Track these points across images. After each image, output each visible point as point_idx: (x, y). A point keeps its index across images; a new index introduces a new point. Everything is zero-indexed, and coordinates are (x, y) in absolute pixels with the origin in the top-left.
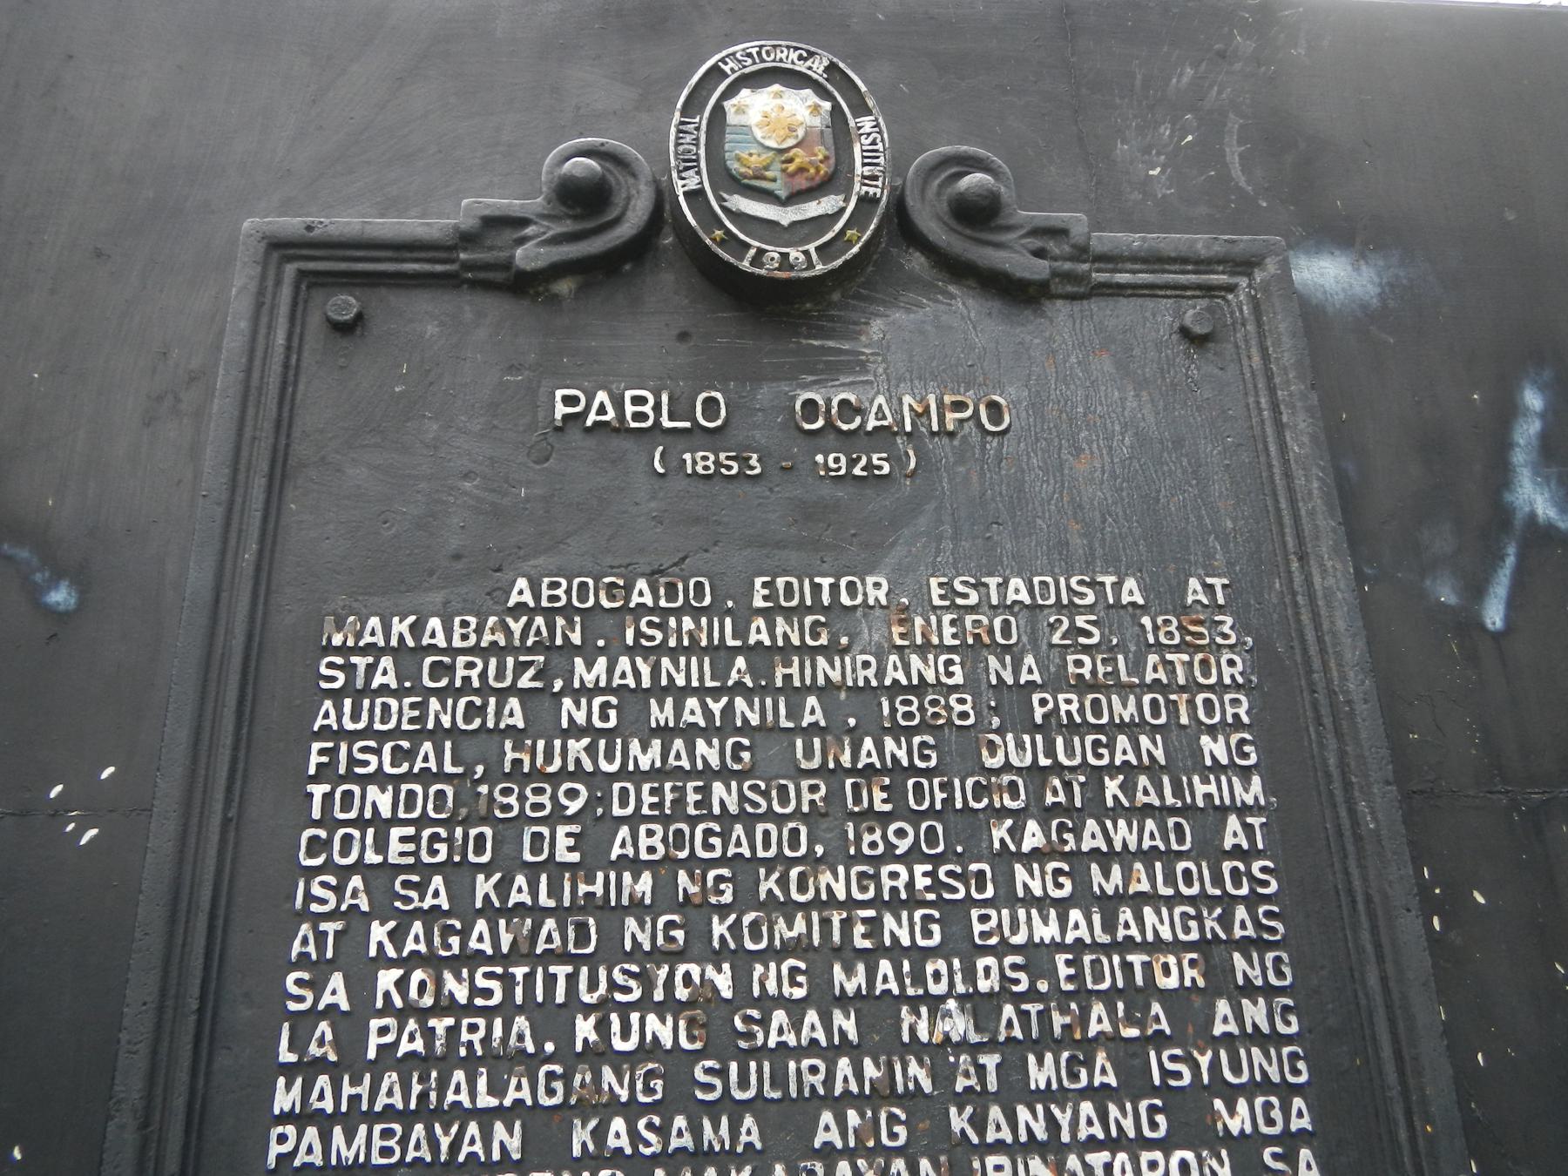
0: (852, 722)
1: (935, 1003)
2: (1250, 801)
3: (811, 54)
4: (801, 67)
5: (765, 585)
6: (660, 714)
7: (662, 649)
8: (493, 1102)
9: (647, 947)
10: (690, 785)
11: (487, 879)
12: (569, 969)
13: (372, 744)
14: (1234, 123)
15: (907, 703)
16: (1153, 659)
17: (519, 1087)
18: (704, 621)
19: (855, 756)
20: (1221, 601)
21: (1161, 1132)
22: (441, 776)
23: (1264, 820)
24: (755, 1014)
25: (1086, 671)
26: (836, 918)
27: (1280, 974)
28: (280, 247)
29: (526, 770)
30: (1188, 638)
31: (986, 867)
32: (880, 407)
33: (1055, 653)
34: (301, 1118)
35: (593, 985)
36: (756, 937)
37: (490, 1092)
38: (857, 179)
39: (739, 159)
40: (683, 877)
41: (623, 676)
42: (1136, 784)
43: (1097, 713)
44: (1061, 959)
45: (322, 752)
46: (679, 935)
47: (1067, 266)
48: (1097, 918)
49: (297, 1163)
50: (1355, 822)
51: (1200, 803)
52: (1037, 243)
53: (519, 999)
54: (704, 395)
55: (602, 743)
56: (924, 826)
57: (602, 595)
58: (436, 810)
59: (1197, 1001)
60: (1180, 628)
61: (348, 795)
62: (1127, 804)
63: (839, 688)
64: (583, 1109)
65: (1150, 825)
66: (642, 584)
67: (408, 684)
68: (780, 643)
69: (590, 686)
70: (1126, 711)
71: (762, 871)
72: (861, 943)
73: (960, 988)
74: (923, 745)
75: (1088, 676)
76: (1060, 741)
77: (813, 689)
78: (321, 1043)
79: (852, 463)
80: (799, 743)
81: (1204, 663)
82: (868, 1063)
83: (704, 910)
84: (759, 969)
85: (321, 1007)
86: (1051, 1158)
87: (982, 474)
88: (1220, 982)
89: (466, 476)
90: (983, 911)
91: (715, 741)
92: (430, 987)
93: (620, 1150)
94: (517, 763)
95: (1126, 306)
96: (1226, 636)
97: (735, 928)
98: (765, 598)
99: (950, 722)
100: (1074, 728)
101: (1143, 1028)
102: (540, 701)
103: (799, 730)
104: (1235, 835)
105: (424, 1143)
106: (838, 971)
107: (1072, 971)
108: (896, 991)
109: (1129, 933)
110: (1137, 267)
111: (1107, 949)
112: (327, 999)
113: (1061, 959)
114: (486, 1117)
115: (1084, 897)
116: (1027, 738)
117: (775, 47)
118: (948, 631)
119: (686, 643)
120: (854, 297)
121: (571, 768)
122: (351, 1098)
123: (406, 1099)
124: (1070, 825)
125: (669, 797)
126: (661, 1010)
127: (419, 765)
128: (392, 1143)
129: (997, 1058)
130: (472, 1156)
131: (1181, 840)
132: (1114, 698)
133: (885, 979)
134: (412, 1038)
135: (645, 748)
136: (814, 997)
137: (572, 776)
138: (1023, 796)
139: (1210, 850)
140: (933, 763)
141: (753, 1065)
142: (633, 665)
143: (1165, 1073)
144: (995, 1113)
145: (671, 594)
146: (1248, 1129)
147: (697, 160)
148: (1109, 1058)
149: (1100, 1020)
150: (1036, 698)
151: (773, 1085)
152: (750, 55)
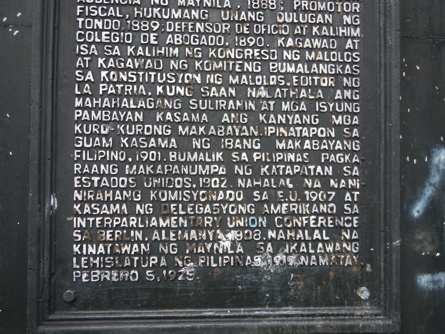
0: (239, 7)
1: (258, 87)
2: (355, 35)
8: (135, 107)
9: (177, 68)
11: (131, 47)
12: (155, 73)
13: (95, 7)
17: (142, 103)
21: (317, 123)
22: (116, 17)
23: (359, 41)
24: (207, 88)
26: (231, 63)
27: (356, 84)
29: (141, 16)
31: (275, 51)
34: (83, 108)
35: (161, 78)
36: (208, 67)
37: (134, 104)
40: (187, 50)
42: (322, 29)
43: (313, 7)
44: (294, 77)
45: (81, 9)
46: (186, 65)
49: (83, 119)
50: (385, 42)
51: (341, 35)
53: (141, 81)
55: (164, 10)
56: (258, 38)
58: (115, 27)
59: (332, 90)
61: (89, 22)
64: (159, 110)
65: (325, 41)
71: (210, 49)
72: (238, 70)
74: (260, 14)
76: (301, 15)
78: (87, 89)
80: (223, 12)
83: (194, 59)
84: (208, 76)
85: (86, 80)
86: (286, 128)
90: (273, 63)
91: (197, 11)
92: (116, 76)
93: (169, 120)
94: (138, 14)
97: (202, 64)
99: (268, 8)
100: (306, 11)
105: (116, 116)
106: (231, 77)
107: (297, 80)
108: (247, 83)
109: (314, 71)
111: (308, 75)
112: (87, 78)
113: (294, 77)
114: (133, 110)
115: (303, 60)
116: (291, 14)
121: (154, 17)
122: (96, 104)
123: (111, 104)
124: (301, 40)
125: (183, 26)
126: (181, 85)
128: (108, 116)
129: (274, 102)
130: (129, 120)
131: (333, 45)
133: (244, 80)
134: (112, 89)
135: (176, 12)
136: (224, 84)
138: (288, 31)
139: (341, 49)
140: (262, 20)
141: (206, 101)
143: (320, 108)
144: (272, 116)
146: (341, 123)
148: (305, 104)
149: (303, 94)
151: (211, 106)
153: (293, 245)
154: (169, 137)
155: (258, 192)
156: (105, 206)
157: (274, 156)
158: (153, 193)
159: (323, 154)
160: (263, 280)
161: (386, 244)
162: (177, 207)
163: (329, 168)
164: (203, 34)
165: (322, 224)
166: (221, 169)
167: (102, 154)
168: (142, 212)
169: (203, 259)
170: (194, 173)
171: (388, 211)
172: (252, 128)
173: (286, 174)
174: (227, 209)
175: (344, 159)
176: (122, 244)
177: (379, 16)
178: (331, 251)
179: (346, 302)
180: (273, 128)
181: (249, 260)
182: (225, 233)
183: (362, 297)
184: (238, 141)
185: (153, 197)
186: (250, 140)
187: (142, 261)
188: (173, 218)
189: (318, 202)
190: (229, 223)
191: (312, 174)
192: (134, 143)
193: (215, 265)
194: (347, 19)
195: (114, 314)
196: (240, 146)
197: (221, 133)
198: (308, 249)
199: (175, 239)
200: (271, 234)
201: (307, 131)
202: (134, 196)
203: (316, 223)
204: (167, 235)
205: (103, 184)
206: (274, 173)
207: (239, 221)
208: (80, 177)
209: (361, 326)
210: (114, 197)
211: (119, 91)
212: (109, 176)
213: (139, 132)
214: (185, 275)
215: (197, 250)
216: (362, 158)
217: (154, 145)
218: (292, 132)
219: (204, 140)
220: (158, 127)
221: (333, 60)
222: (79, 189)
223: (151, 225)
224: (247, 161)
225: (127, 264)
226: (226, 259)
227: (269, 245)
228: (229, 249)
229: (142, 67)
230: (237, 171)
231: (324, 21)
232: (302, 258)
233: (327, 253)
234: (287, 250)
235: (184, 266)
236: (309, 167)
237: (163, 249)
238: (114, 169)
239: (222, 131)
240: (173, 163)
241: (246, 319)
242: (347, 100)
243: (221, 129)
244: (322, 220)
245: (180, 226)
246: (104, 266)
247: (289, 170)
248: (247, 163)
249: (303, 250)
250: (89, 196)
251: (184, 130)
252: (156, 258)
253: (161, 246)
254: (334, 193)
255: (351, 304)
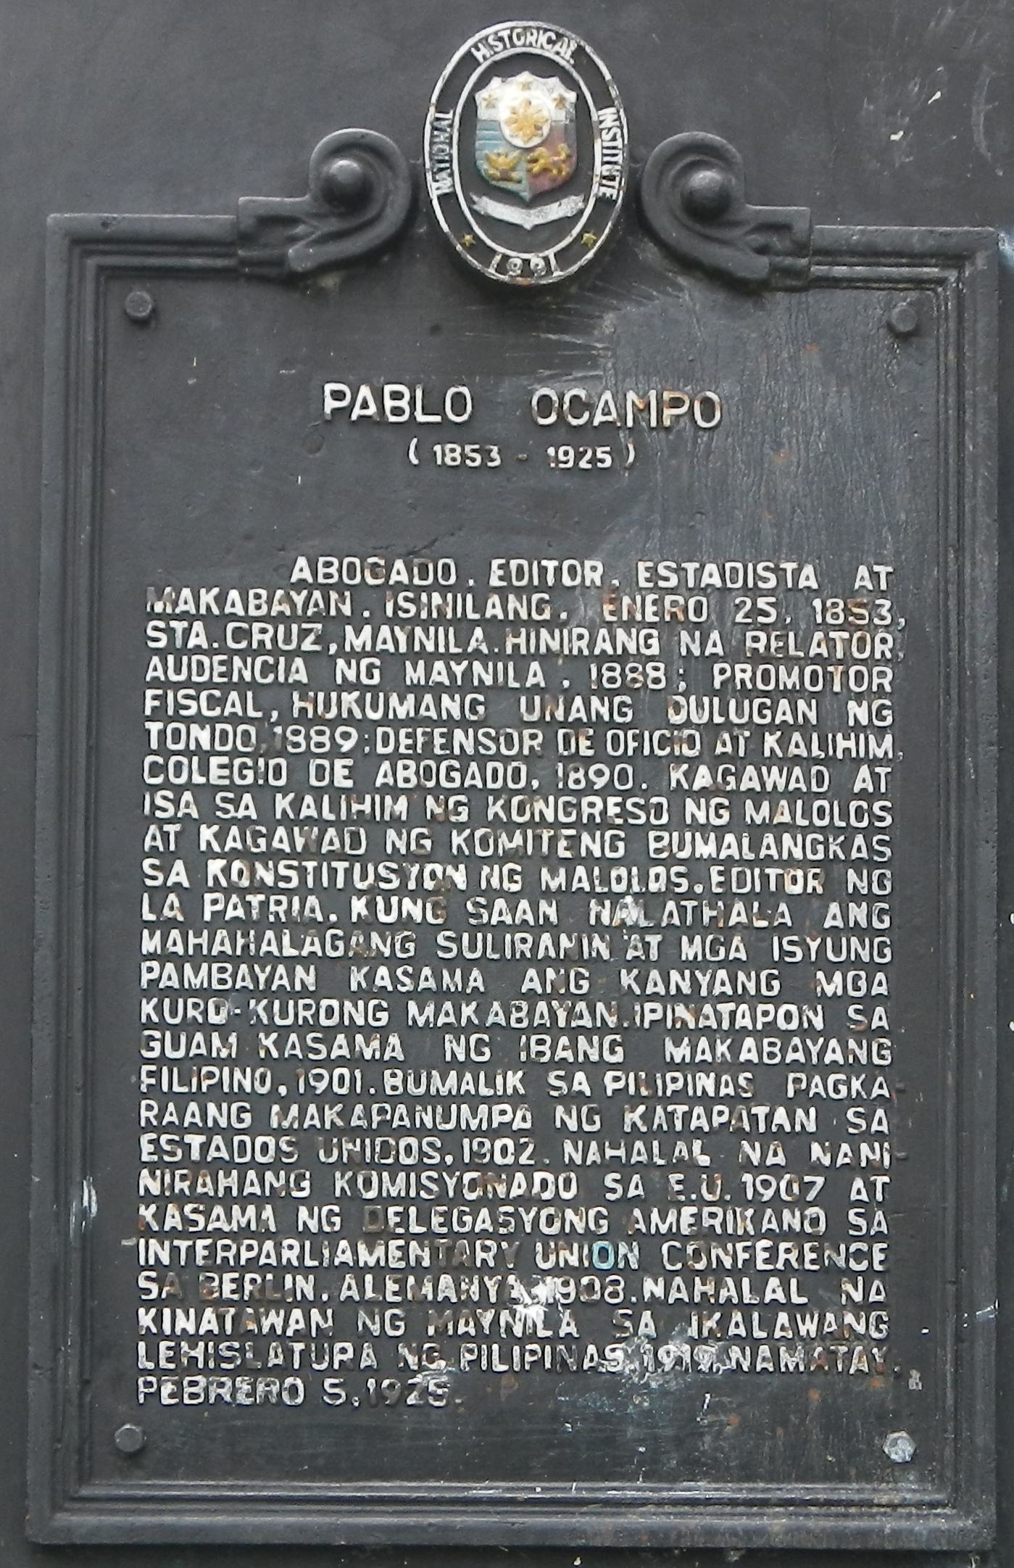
1: (616, 898)
2: (880, 754)
3: (559, 36)
4: (549, 52)
5: (500, 567)
6: (414, 674)
7: (416, 620)
8: (294, 953)
9: (403, 851)
10: (437, 731)
11: (284, 797)
12: (346, 864)
13: (192, 692)
14: (987, 75)
15: (611, 669)
16: (818, 636)
17: (312, 944)
18: (450, 596)
19: (567, 711)
20: (883, 586)
21: (775, 992)
22: (246, 720)
23: (889, 770)
24: (482, 901)
25: (761, 647)
26: (546, 835)
27: (882, 886)
28: (82, 243)
29: (310, 715)
30: (851, 619)
31: (664, 801)
32: (606, 402)
33: (737, 630)
34: (163, 957)
35: (364, 877)
38: (596, 179)
39: (488, 159)
41: (385, 642)
43: (766, 680)
45: (155, 698)
47: (788, 261)
48: (746, 842)
49: (161, 986)
50: (960, 774)
51: (840, 755)
52: (758, 239)
53: (310, 884)
54: (452, 391)
55: (369, 696)
56: (618, 768)
57: (367, 573)
59: (816, 903)
60: (846, 609)
61: (177, 733)
62: (780, 755)
63: (557, 655)
64: (359, 960)
65: (797, 771)
66: (399, 564)
67: (216, 645)
68: (511, 617)
69: (358, 650)
70: (789, 680)
71: (491, 799)
72: (563, 853)
73: (636, 888)
74: (622, 704)
75: (762, 650)
76: (733, 703)
77: (536, 656)
78: (172, 908)
79: (579, 456)
80: (523, 700)
81: (862, 640)
82: (563, 937)
84: (486, 870)
85: (169, 883)
87: (692, 467)
88: (835, 890)
89: (254, 464)
90: (659, 833)
91: (457, 697)
92: (246, 873)
94: (303, 711)
95: (841, 296)
96: (883, 618)
97: (470, 840)
98: (501, 578)
99: (645, 685)
100: (746, 693)
101: (771, 920)
102: (320, 662)
103: (523, 690)
104: (864, 781)
105: (248, 978)
106: (544, 871)
107: (722, 879)
108: (587, 889)
109: (769, 852)
110: (855, 260)
113: (714, 870)
114: (290, 962)
115: (737, 825)
116: (706, 700)
117: (525, 28)
118: (650, 609)
119: (435, 615)
120: (589, 290)
121: (345, 715)
123: (234, 948)
124: (733, 770)
125: (420, 740)
126: (413, 895)
127: (228, 710)
128: (225, 976)
129: (659, 938)
130: (282, 986)
131: (820, 784)
132: (782, 668)
134: (235, 908)
135: (402, 700)
137: (345, 722)
139: (842, 793)
140: (629, 719)
141: (480, 936)
142: (392, 632)
144: (655, 975)
145: (424, 576)
146: (840, 992)
147: (451, 161)
148: (742, 940)
149: (739, 914)
150: (717, 667)
152: (501, 39)
153: (710, 1317)
154: (384, 1032)
155: (618, 1176)
156: (218, 1210)
157: (659, 1082)
158: (343, 1176)
159: (791, 1076)
160: (631, 1409)
161: (959, 1317)
162: (404, 1216)
163: (807, 1113)
164: (472, 758)
165: (787, 1261)
166: (519, 1114)
167: (211, 1075)
168: (314, 1228)
169: (471, 1351)
170: (448, 1127)
171: (965, 1227)
172: (600, 1007)
173: (692, 1128)
174: (536, 1222)
175: (849, 1089)
176: (262, 1310)
177: (948, 704)
178: (813, 1335)
179: (853, 1472)
180: (658, 1006)
181: (592, 1356)
182: (529, 1284)
183: (893, 1457)
184: (564, 1040)
185: (343, 1189)
186: (596, 1039)
187: (313, 1355)
188: (393, 1244)
189: (777, 1204)
190: (539, 1258)
191: (762, 1128)
192: (294, 1047)
193: (504, 1368)
194: (858, 712)
195: (243, 1488)
196: (568, 1055)
197: (519, 1020)
198: (749, 1329)
199: (398, 1299)
200: (652, 1287)
201: (748, 1014)
202: (292, 1185)
203: (772, 1259)
204: (379, 1287)
205: (212, 1154)
206: (660, 1126)
207: (567, 1253)
208: (154, 1136)
209: (887, 1531)
210: (241, 1188)
211: (255, 913)
212: (229, 1133)
213: (305, 1019)
214: (425, 1392)
215: (456, 1328)
216: (900, 1086)
217: (345, 1052)
218: (707, 1018)
219: (473, 1038)
220: (356, 1006)
221: (818, 822)
222: (152, 1167)
223: (337, 1263)
224: (588, 1093)
225: (276, 1361)
226: (533, 1352)
227: (646, 1317)
228: (540, 1325)
229: (313, 849)
230: (562, 1121)
231: (795, 717)
232: (735, 1352)
233: (802, 1339)
234: (693, 1332)
235: (421, 1368)
236: (754, 1111)
237: (368, 1322)
238: (243, 1116)
239: (523, 1014)
240: (394, 1100)
241: (584, 1509)
242: (857, 930)
243: (519, 1009)
244: (788, 1251)
245: (413, 1263)
246: (217, 1365)
247: (699, 1118)
248: (588, 1099)
249: (737, 1332)
250: (179, 1185)
251: (421, 1013)
252: (349, 1346)
253: (363, 1316)
254: (820, 1181)
255: (865, 1476)
